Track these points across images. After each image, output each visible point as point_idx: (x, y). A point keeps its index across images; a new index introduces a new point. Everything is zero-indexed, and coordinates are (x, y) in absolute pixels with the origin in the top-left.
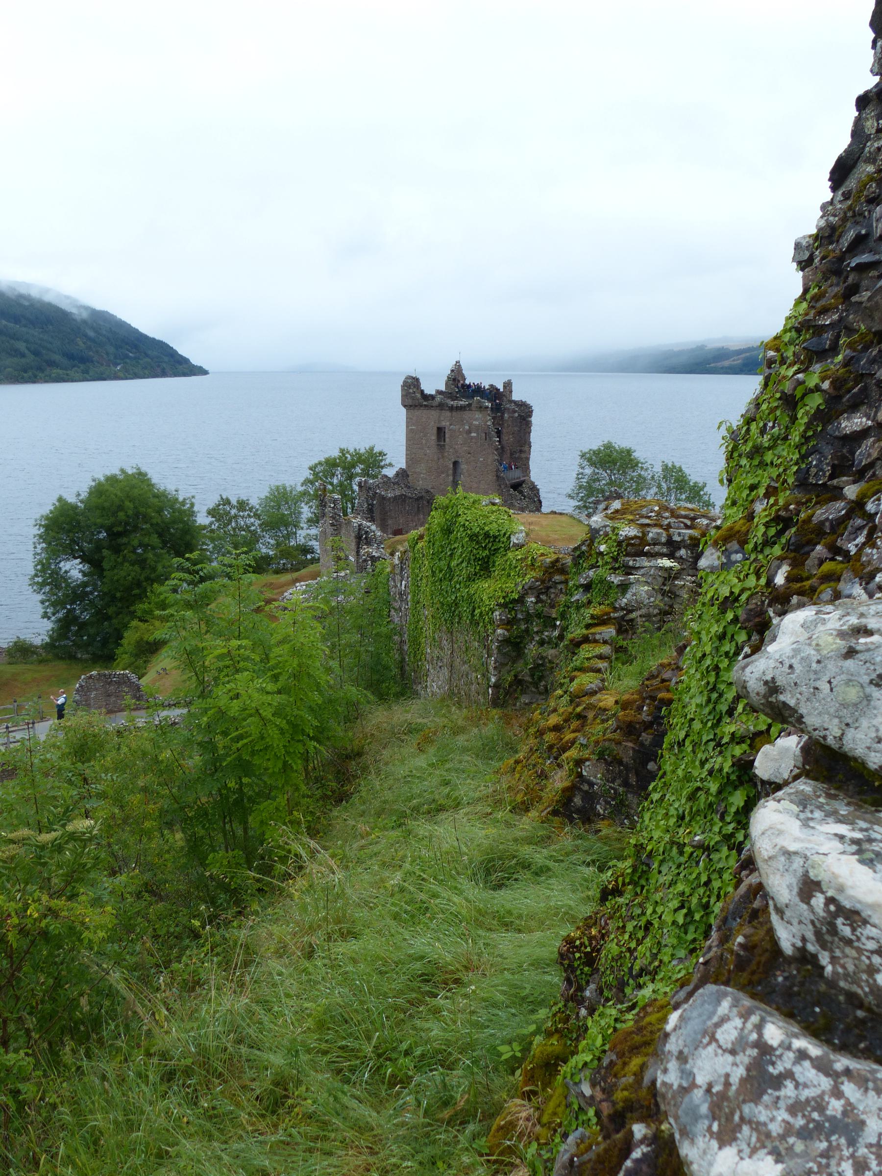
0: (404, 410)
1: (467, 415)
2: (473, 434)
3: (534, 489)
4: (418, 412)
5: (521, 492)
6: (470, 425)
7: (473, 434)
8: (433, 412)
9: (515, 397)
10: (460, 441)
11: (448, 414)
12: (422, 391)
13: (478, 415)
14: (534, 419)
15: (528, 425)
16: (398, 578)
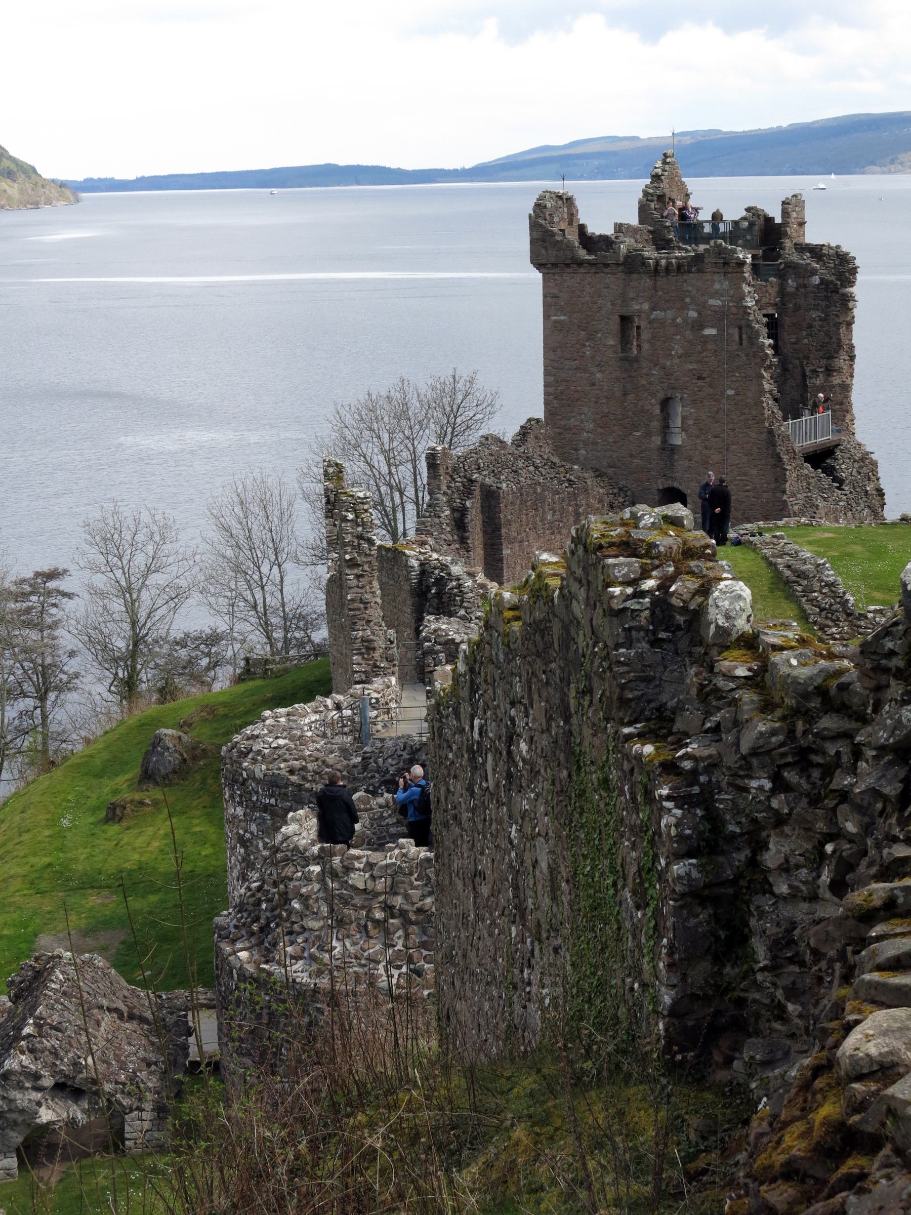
0: (537, 276)
1: (692, 283)
2: (710, 331)
3: (867, 465)
5: (830, 471)
6: (702, 308)
7: (710, 331)
8: (609, 279)
9: (812, 236)
10: (677, 349)
11: (647, 282)
12: (582, 228)
13: (720, 284)
14: (862, 290)
15: (846, 303)
16: (465, 709)
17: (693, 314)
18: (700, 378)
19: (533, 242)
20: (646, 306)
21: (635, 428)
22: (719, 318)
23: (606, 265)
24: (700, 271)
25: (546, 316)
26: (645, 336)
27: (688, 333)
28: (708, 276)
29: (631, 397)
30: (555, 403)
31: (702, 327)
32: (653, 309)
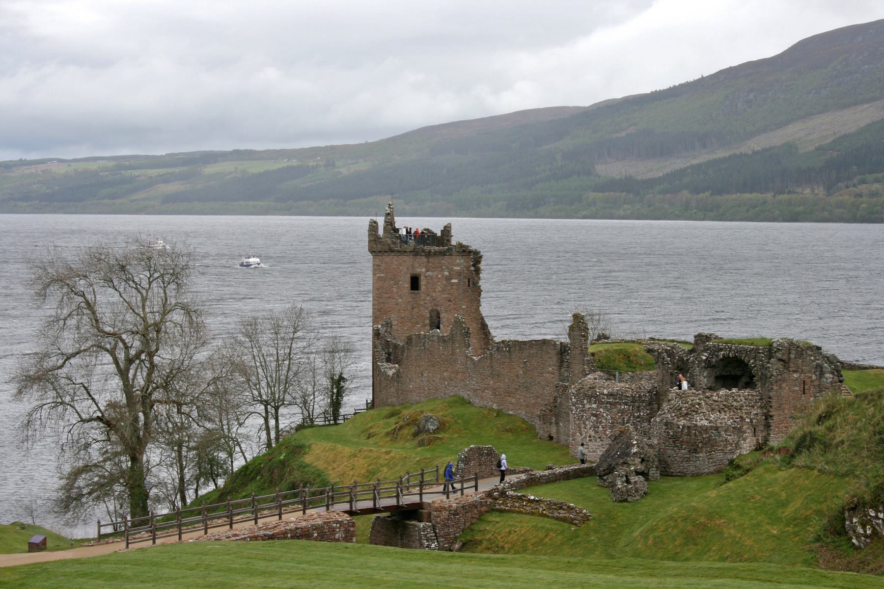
4: (387, 259)
6: (451, 271)
8: (405, 258)
10: (439, 288)
11: (424, 259)
17: (446, 273)
18: (450, 301)
19: (370, 241)
20: (424, 270)
21: (417, 323)
22: (459, 274)
23: (405, 252)
24: (450, 255)
25: (374, 274)
26: (423, 282)
27: (444, 282)
28: (454, 257)
29: (416, 310)
30: (378, 313)
31: (451, 279)
32: (427, 271)
